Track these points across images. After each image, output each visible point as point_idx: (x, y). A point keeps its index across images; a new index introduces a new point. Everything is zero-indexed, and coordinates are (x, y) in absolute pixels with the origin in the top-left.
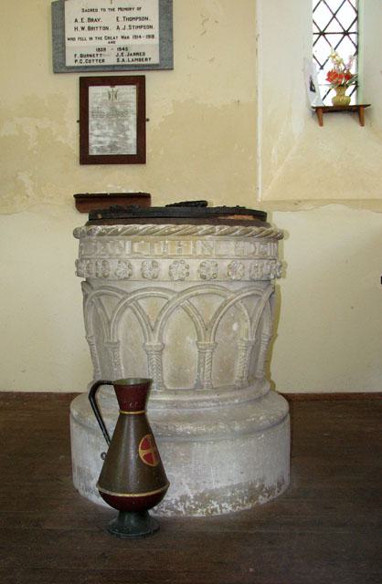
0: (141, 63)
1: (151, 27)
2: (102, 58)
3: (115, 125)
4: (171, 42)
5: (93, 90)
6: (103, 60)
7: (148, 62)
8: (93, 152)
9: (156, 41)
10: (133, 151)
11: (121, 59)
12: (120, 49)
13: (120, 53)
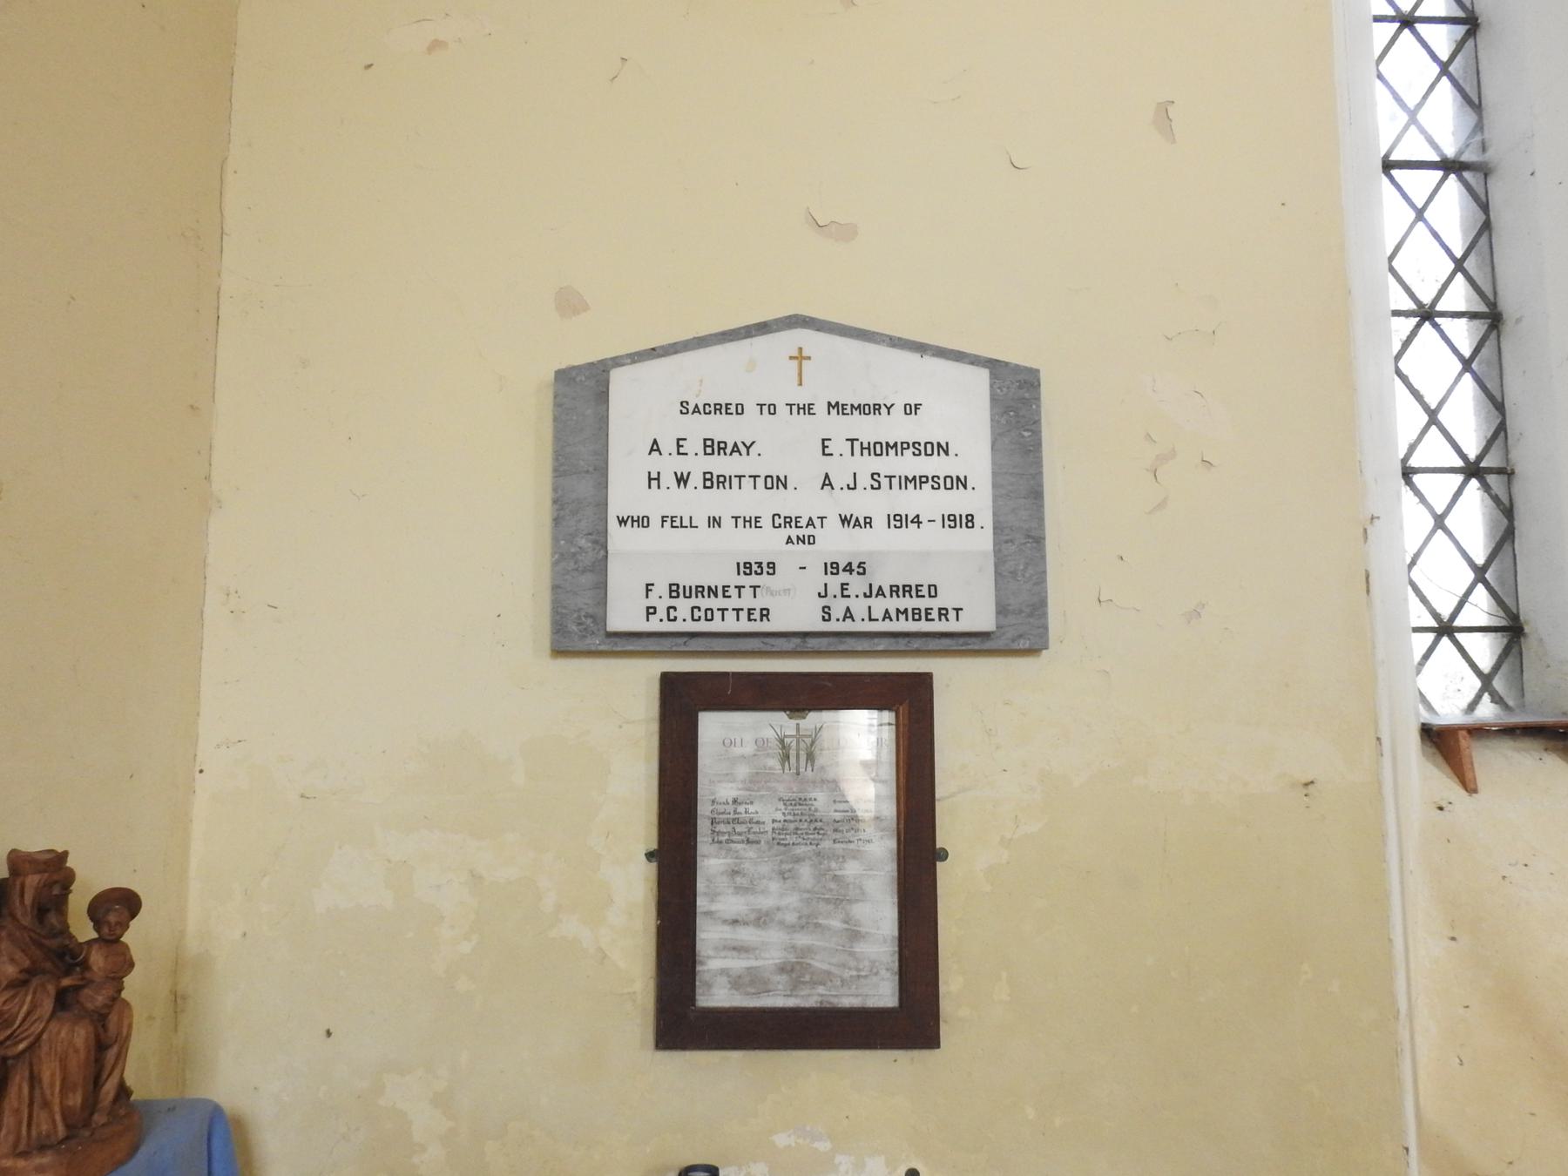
0: (923, 626)
1: (961, 482)
2: (758, 604)
3: (806, 872)
4: (1038, 541)
5: (713, 727)
6: (765, 614)
7: (951, 626)
8: (716, 994)
9: (981, 539)
10: (883, 993)
11: (838, 611)
12: (833, 568)
13: (834, 583)
